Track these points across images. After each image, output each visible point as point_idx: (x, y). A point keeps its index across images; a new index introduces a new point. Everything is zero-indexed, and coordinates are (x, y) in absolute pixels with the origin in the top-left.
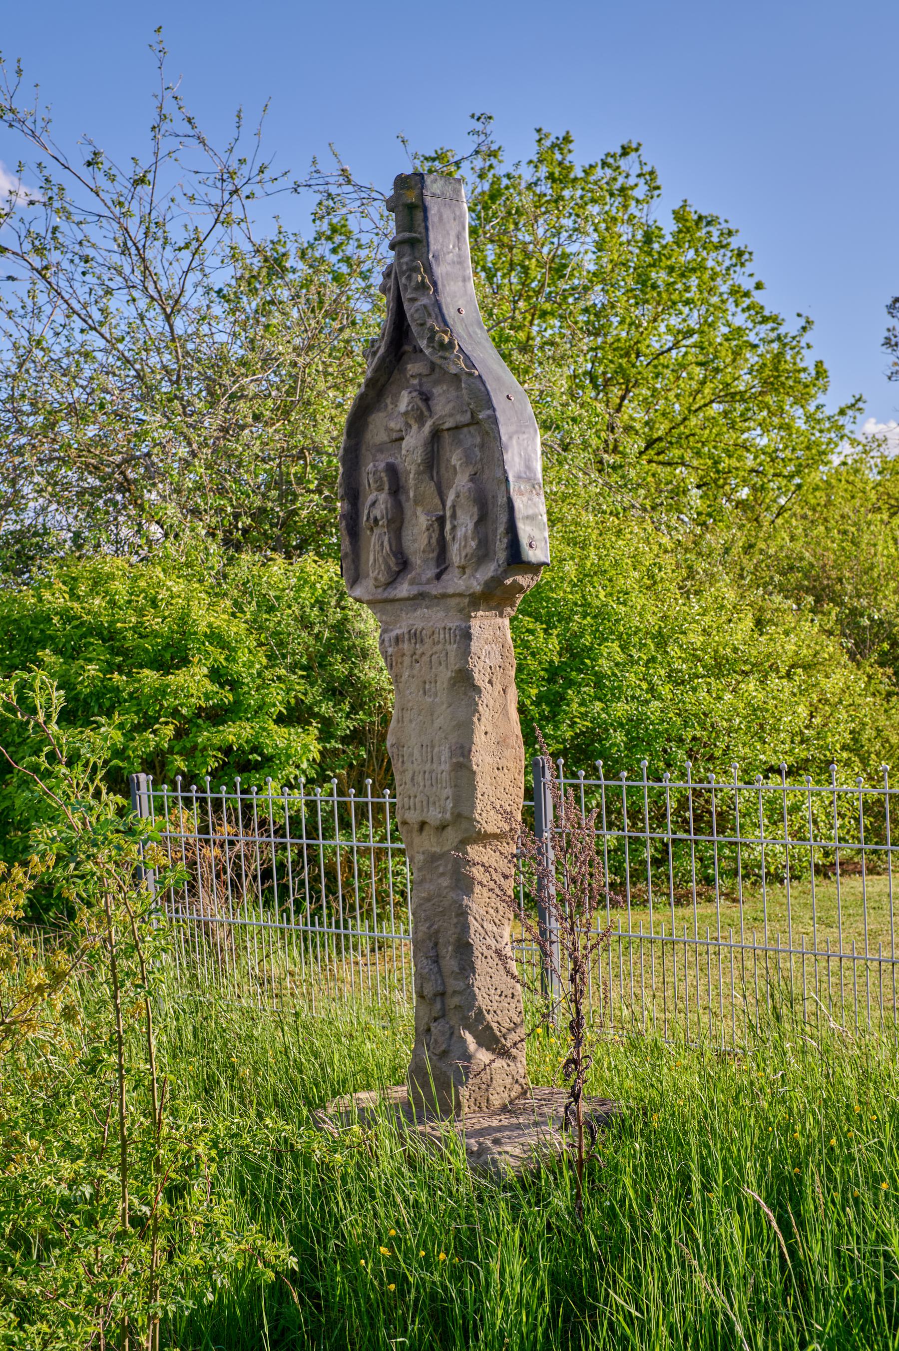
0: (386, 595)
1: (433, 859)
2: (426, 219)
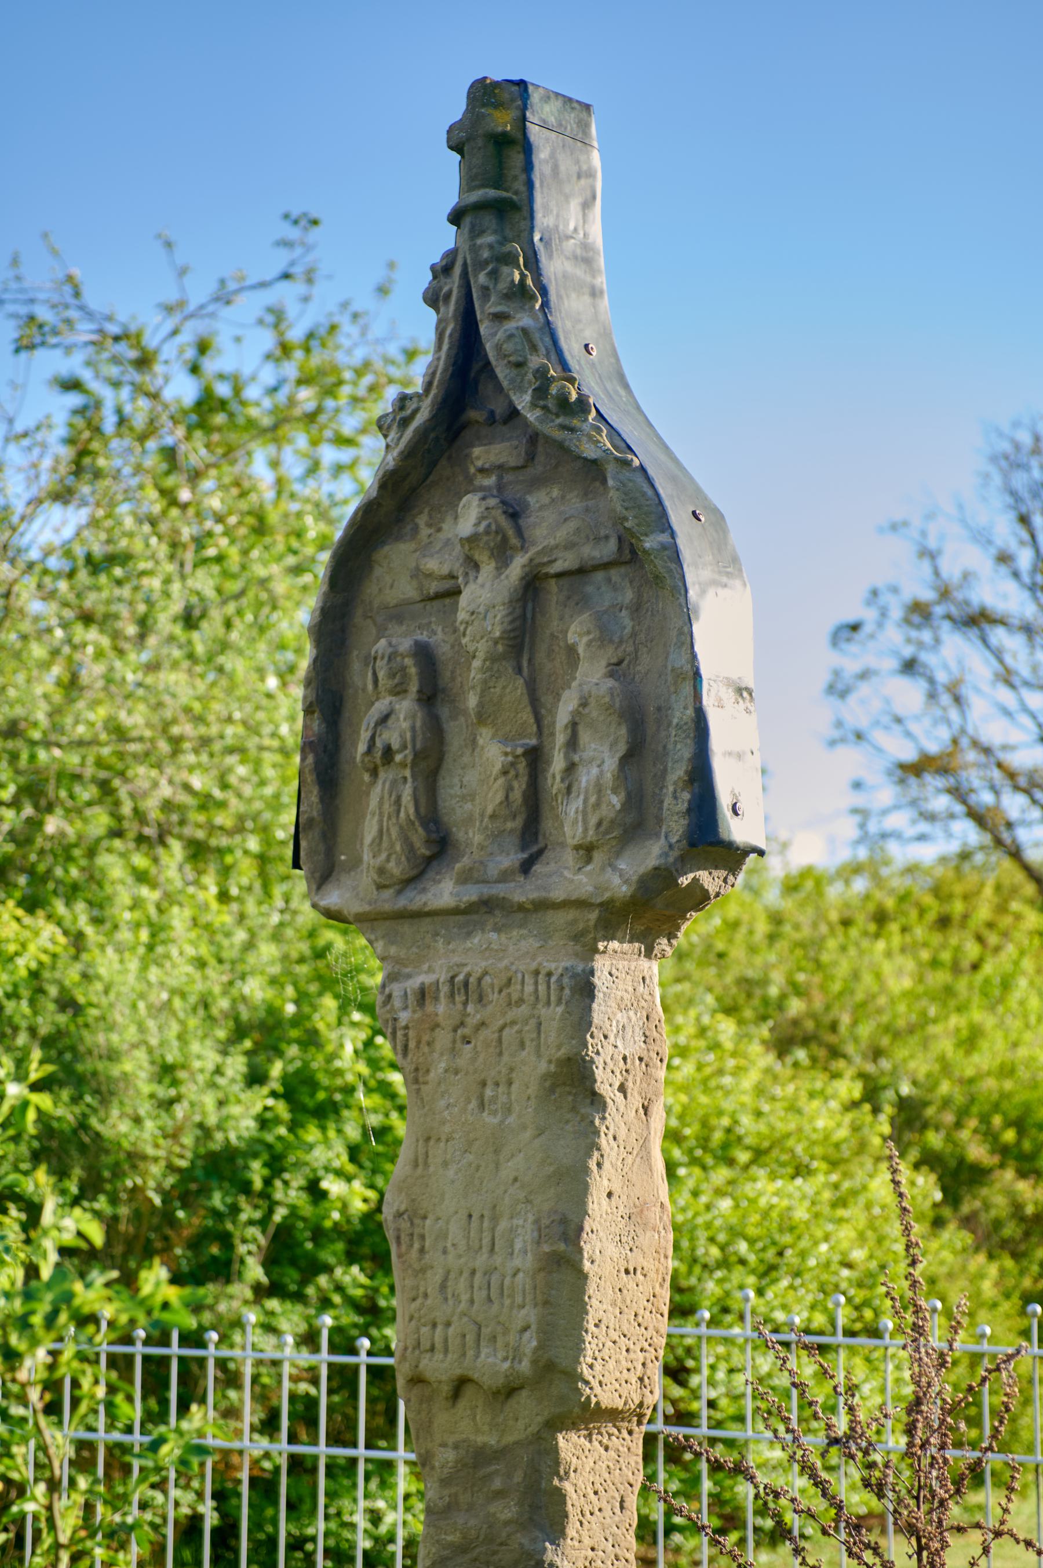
0: (402, 903)
1: (477, 1460)
2: (528, 167)
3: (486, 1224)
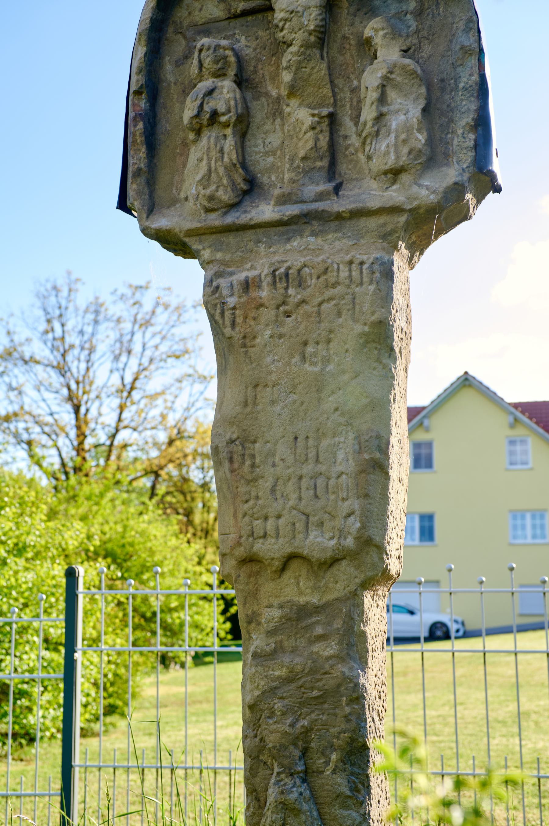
0: (230, 219)
3: (311, 442)
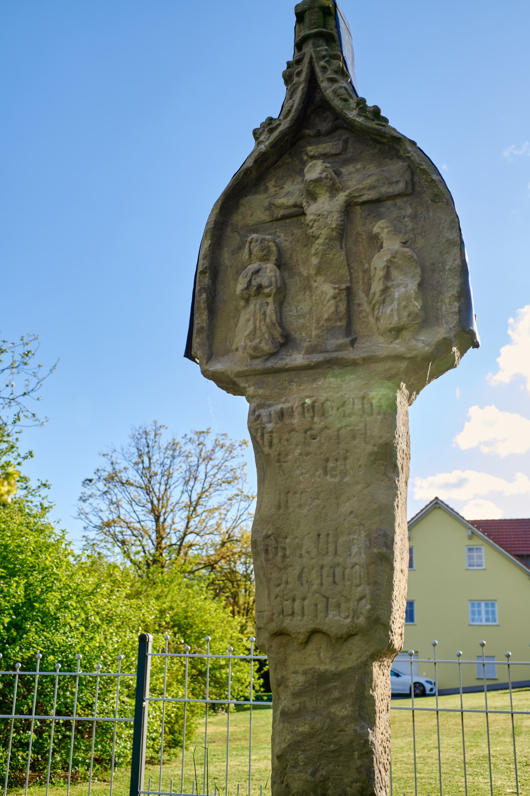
0: (269, 364)
3: (331, 539)
